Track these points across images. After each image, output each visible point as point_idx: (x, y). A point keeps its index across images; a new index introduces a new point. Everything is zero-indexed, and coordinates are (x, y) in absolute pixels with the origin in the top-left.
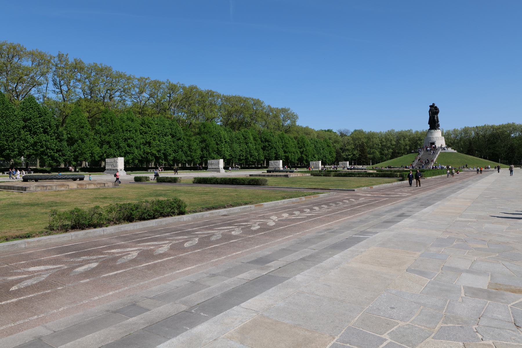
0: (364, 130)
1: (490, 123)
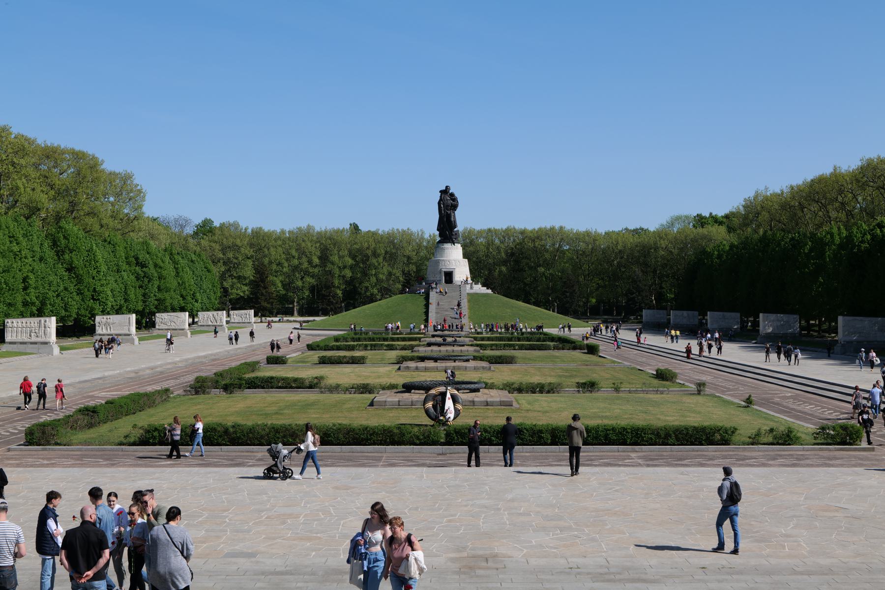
0: (243, 225)
1: (519, 225)
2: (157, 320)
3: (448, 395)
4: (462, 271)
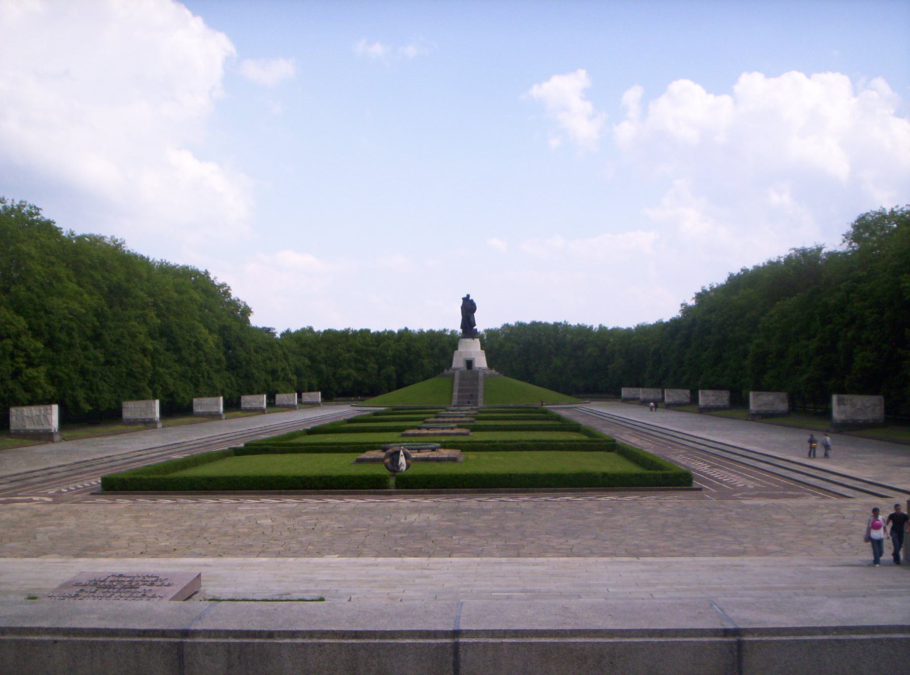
2: (242, 401)
3: (402, 453)
4: (481, 362)
